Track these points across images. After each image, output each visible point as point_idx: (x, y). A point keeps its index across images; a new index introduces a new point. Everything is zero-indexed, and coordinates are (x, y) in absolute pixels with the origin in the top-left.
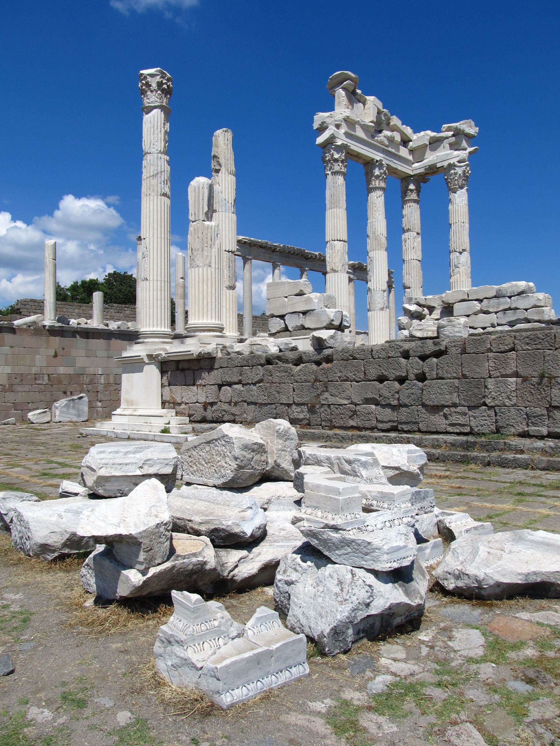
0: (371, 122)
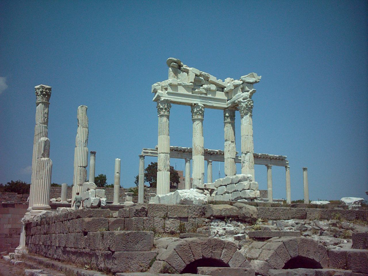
0: (191, 82)
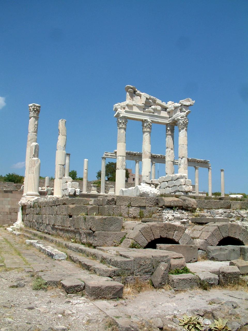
0: (143, 104)
